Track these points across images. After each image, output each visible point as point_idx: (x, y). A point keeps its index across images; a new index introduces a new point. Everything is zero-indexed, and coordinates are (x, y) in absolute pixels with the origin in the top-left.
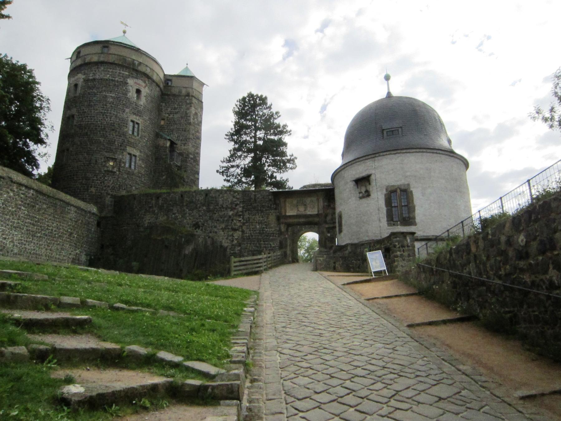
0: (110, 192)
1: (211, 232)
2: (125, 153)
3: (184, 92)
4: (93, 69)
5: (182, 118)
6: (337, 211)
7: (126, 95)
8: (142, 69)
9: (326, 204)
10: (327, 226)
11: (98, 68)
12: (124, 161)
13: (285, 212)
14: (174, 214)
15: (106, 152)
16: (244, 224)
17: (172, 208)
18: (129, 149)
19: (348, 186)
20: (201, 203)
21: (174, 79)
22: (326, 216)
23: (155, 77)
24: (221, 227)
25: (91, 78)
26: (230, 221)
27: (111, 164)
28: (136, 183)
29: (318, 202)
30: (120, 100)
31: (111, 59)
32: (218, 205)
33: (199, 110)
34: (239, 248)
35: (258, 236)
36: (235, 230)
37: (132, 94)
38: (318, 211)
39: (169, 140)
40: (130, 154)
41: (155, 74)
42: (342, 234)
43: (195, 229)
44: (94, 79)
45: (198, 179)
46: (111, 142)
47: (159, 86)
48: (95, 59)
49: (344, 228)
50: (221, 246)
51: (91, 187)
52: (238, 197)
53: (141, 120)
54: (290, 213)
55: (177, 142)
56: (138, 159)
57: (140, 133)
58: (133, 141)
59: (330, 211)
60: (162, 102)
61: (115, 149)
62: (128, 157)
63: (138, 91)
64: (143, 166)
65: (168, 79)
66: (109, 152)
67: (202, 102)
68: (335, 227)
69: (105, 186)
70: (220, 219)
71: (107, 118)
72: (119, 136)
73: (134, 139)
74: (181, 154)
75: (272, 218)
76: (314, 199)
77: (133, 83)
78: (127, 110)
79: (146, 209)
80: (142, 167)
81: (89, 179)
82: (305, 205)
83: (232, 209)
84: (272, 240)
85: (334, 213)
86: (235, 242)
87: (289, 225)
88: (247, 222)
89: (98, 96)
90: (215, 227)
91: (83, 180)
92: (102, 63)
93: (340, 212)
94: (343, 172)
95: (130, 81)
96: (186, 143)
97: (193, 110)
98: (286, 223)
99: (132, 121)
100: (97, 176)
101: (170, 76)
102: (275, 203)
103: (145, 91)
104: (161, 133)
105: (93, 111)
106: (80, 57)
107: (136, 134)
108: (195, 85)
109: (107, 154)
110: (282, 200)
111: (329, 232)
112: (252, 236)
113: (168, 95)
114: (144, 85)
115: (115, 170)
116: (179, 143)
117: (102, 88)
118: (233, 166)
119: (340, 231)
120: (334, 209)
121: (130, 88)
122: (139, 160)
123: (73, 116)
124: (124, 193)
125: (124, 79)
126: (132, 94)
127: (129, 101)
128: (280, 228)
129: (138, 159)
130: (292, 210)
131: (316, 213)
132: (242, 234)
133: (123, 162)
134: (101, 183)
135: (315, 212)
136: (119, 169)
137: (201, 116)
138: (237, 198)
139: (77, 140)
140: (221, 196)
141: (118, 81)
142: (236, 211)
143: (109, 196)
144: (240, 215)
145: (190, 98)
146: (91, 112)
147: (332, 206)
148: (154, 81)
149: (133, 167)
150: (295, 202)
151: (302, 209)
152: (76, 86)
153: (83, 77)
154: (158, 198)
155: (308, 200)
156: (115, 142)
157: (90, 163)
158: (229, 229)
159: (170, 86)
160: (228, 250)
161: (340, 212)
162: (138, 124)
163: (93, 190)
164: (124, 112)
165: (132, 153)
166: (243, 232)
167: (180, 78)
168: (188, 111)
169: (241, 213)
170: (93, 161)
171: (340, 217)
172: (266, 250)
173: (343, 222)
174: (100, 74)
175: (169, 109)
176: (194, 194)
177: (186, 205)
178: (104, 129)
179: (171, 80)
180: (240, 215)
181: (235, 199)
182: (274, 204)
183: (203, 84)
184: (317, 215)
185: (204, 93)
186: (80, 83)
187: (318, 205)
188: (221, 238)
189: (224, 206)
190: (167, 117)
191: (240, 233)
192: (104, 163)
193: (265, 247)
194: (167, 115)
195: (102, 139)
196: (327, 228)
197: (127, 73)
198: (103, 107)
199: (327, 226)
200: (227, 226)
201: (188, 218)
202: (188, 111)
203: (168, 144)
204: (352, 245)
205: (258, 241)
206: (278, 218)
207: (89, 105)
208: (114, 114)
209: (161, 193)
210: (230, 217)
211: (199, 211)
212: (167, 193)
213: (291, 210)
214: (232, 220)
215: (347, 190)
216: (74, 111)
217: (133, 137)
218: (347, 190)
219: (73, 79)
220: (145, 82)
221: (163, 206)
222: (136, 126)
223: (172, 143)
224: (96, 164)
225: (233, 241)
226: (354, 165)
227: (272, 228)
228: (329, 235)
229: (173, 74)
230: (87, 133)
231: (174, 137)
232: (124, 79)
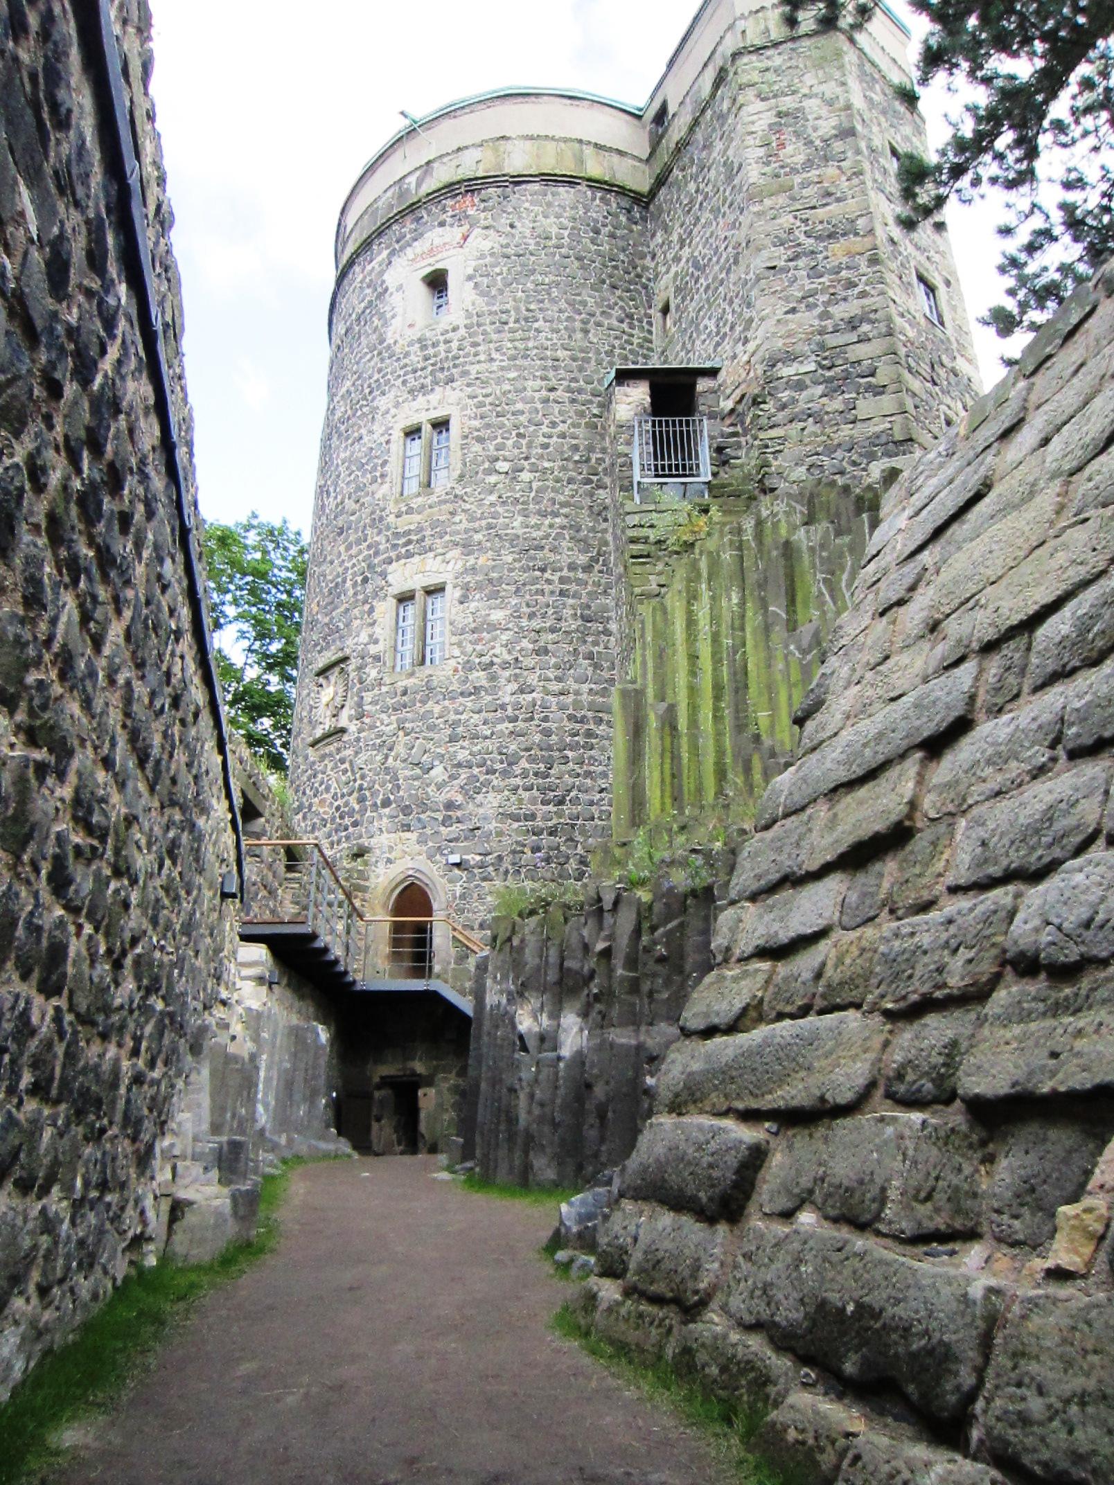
64: (497, 616)
80: (492, 627)
101: (652, 98)
148: (518, 181)
165: (417, 583)
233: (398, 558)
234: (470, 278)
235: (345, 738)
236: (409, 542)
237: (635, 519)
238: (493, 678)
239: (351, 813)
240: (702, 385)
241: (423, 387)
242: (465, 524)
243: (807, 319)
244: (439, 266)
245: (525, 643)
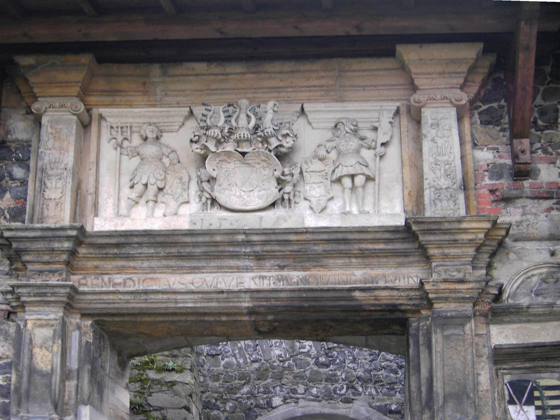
9: (485, 156)
10: (503, 335)
13: (82, 200)
22: (496, 245)
29: (418, 140)
76: (374, 111)
82: (282, 157)
184: (411, 238)
196: (501, 356)
199: (503, 335)
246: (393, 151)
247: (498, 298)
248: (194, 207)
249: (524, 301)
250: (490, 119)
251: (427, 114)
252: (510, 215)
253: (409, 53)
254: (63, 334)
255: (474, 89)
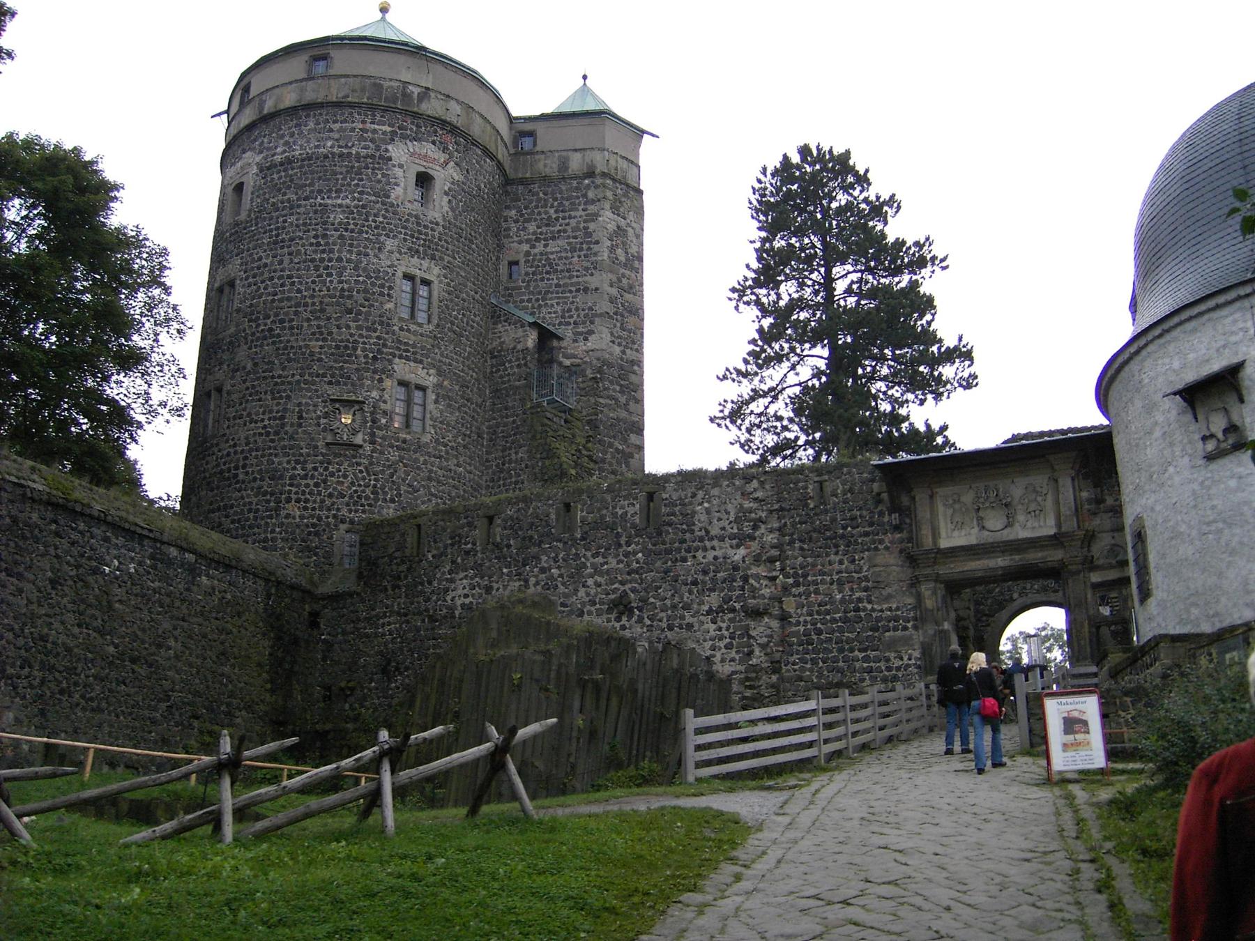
0: (344, 512)
1: (670, 628)
2: (388, 383)
3: (576, 163)
4: (285, 130)
5: (573, 250)
6: (1128, 520)
7: (388, 197)
8: (432, 107)
9: (1085, 494)
11: (298, 125)
12: (387, 407)
13: (935, 534)
14: (543, 570)
15: (330, 383)
16: (785, 589)
17: (536, 549)
18: (402, 368)
19: (1160, 418)
20: (634, 526)
21: (540, 128)
22: (1090, 538)
23: (477, 129)
24: (706, 608)
25: (278, 158)
26: (739, 583)
27: (347, 419)
28: (430, 479)
29: (1057, 492)
30: (367, 214)
31: (335, 92)
32: (692, 532)
33: (631, 216)
34: (774, 678)
35: (841, 630)
36: (757, 614)
37: (403, 191)
38: (1059, 525)
39: (535, 325)
40: (402, 383)
41: (479, 120)
42: (1152, 602)
43: (618, 619)
44: (289, 161)
45: (640, 448)
46: (345, 351)
47: (492, 157)
48: (289, 98)
49: (1157, 579)
50: (711, 676)
51: (288, 501)
52: (759, 494)
53: (436, 271)
54: (951, 538)
55: (559, 332)
56: (432, 397)
57: (435, 311)
58: (412, 339)
59: (1101, 522)
60: (508, 207)
61: (357, 370)
62: (401, 392)
63: (424, 180)
65: (525, 129)
66: (338, 383)
67: (640, 192)
68: (1127, 581)
69: (330, 495)
70: (700, 577)
71: (330, 275)
72: (368, 329)
73: (415, 333)
74: (573, 371)
75: (889, 563)
76: (1040, 480)
77: (404, 157)
78: (390, 244)
79: (453, 562)
81: (281, 477)
83: (741, 539)
84: (891, 645)
85: (1121, 529)
86: (758, 658)
87: (953, 587)
88: (797, 584)
89: (303, 210)
90: (687, 607)
91: (262, 480)
92: (309, 107)
93: (1139, 519)
94: (1134, 366)
95: (398, 152)
96: (591, 332)
97: (608, 219)
98: (937, 579)
99: (409, 277)
100: (305, 462)
102: (895, 508)
103: (445, 175)
104: (510, 307)
105: (286, 259)
106: (250, 101)
107: (421, 317)
108: (612, 139)
109: (333, 392)
110: (921, 496)
111: (1104, 601)
112: (819, 632)
113: (523, 182)
114: (442, 157)
115: (358, 439)
116: (567, 332)
117: (311, 185)
118: (756, 395)
119: (1145, 594)
120: (1117, 511)
121: (399, 172)
122: (436, 402)
123: (232, 284)
124: (390, 512)
125: (378, 148)
126: (403, 191)
127: (395, 213)
128: (919, 598)
129: (432, 397)
130: (960, 526)
131: (1052, 532)
132: (783, 627)
133: (385, 413)
134: (317, 485)
135: (1048, 527)
136: (373, 435)
137: (639, 236)
138: (756, 499)
139: (242, 353)
140: (701, 494)
141: (358, 156)
142: (755, 545)
143: (343, 527)
144: (772, 560)
145: (599, 181)
146: (281, 262)
147: (1110, 501)
148: (475, 143)
149: (416, 426)
150: (968, 498)
151: (995, 521)
152: (239, 188)
153: (258, 158)
154: (491, 519)
155: (1016, 488)
156: (355, 349)
157: (283, 425)
158: (733, 610)
159: (531, 153)
160: (735, 687)
161: (1139, 519)
162: (426, 282)
163: (293, 509)
164: (380, 249)
165: (410, 377)
166: (784, 618)
167: (564, 122)
168: (592, 226)
169: (775, 552)
170: (291, 418)
171: (1140, 537)
172: (874, 679)
173: (1152, 558)
174: (306, 141)
175: (532, 227)
176: (608, 497)
177: (583, 539)
178: (322, 310)
179: (531, 134)
180: (772, 560)
181: (747, 505)
182: (892, 510)
183: (639, 133)
184: (1057, 540)
185: (644, 161)
186: (251, 180)
187: (1057, 503)
188: (708, 644)
189: (715, 531)
190: (528, 254)
191: (775, 624)
192: (323, 421)
193: (870, 670)
194: (526, 247)
195: (315, 345)
196: (1095, 586)
197: (389, 129)
198: (318, 244)
199: (1095, 578)
200: (727, 600)
201: (590, 582)
202: (592, 226)
203: (531, 339)
204: (1175, 639)
205: (841, 650)
206: (912, 560)
207: (275, 243)
208: (349, 261)
209: (499, 502)
210: (736, 568)
211: (627, 555)
212: (518, 500)
213: (953, 528)
214: (745, 579)
215: (1157, 433)
216: (234, 267)
217: (413, 327)
218: (1157, 433)
219: (231, 172)
220: (445, 150)
221: (509, 546)
222: (423, 291)
223: (546, 336)
224: (300, 425)
225: (750, 653)
226: (1175, 333)
227: (888, 598)
228: (1106, 611)
229: (537, 112)
230: (271, 330)
231: (549, 318)
232: (378, 148)
233: (401, 357)
234: (446, 193)
235: (361, 451)
236: (407, 351)
237: (549, 415)
238: (447, 452)
239: (367, 498)
240: (555, 343)
241: (417, 251)
242: (438, 357)
243: (617, 350)
244: (430, 171)
245: (460, 440)
246: (1049, 497)
247: (1092, 562)
248: (976, 530)
249: (1101, 562)
250: (1086, 477)
251: (1061, 482)
252: (1097, 522)
253: (1051, 458)
254: (934, 593)
255: (1077, 467)
